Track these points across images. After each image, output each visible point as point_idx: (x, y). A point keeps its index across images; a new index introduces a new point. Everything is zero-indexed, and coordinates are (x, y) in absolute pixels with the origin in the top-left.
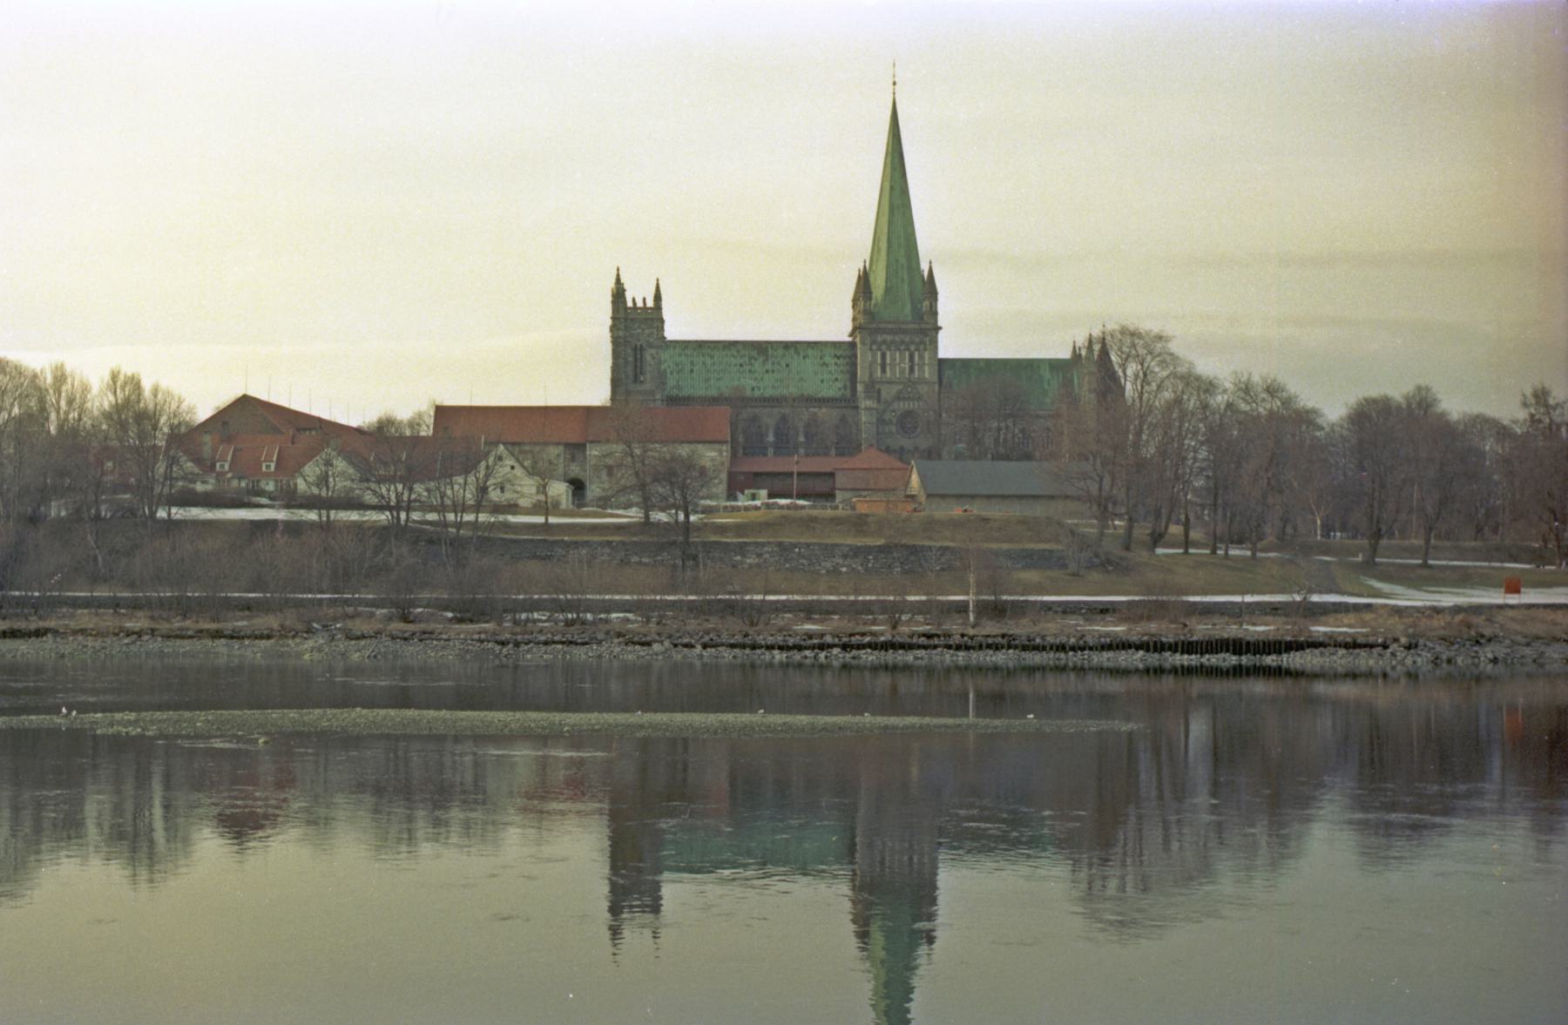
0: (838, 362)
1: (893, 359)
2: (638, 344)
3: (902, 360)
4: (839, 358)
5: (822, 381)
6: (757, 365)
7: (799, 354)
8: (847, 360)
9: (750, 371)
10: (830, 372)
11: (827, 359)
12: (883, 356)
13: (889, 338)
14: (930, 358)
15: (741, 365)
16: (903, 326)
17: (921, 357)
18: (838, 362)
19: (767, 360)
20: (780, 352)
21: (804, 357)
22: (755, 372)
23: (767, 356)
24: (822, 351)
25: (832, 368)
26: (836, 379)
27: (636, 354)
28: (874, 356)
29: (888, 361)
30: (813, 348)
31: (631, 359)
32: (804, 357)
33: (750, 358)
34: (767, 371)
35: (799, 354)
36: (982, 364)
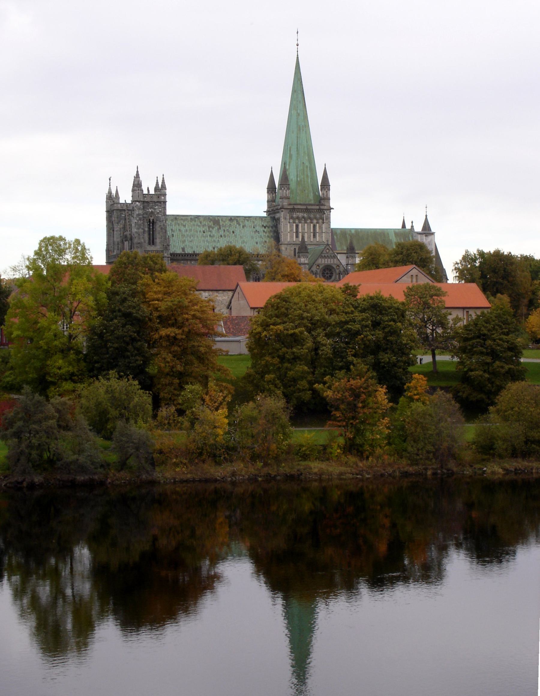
0: (265, 230)
1: (303, 229)
2: (151, 219)
3: (309, 228)
4: (265, 227)
5: (257, 243)
6: (214, 231)
7: (239, 225)
8: (271, 229)
9: (210, 236)
10: (261, 237)
11: (258, 228)
12: (297, 226)
13: (300, 215)
14: (326, 229)
15: (204, 232)
16: (309, 207)
17: (321, 228)
18: (265, 230)
19: (220, 228)
20: (228, 223)
21: (243, 227)
22: (213, 236)
23: (220, 225)
24: (254, 222)
25: (262, 234)
26: (266, 242)
27: (149, 225)
28: (291, 227)
29: (300, 230)
30: (248, 220)
31: (146, 229)
32: (243, 227)
33: (209, 227)
34: (221, 236)
35: (239, 225)
36: (353, 232)
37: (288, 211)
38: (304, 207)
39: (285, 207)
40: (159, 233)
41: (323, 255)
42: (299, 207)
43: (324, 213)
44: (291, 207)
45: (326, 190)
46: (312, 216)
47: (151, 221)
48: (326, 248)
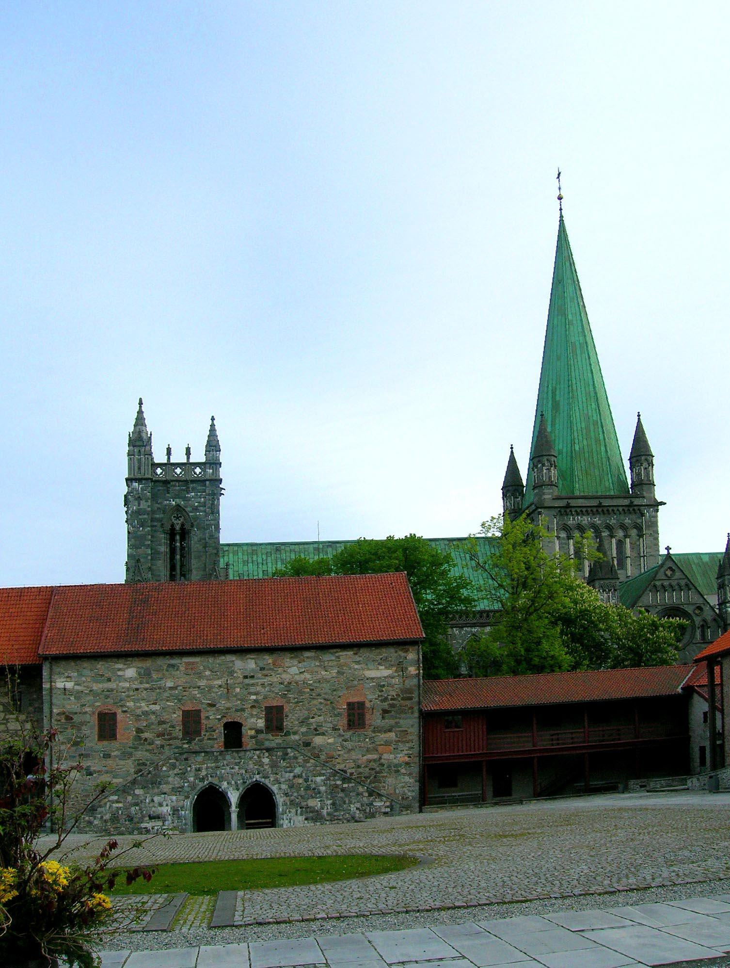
16: (606, 502)
37: (554, 512)
38: (594, 503)
39: (546, 505)
40: (199, 557)
41: (658, 583)
42: (580, 502)
43: (642, 515)
44: (562, 503)
45: (645, 464)
46: (613, 522)
47: (178, 528)
48: (665, 567)
